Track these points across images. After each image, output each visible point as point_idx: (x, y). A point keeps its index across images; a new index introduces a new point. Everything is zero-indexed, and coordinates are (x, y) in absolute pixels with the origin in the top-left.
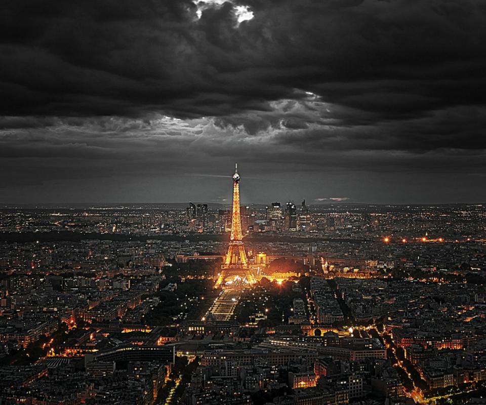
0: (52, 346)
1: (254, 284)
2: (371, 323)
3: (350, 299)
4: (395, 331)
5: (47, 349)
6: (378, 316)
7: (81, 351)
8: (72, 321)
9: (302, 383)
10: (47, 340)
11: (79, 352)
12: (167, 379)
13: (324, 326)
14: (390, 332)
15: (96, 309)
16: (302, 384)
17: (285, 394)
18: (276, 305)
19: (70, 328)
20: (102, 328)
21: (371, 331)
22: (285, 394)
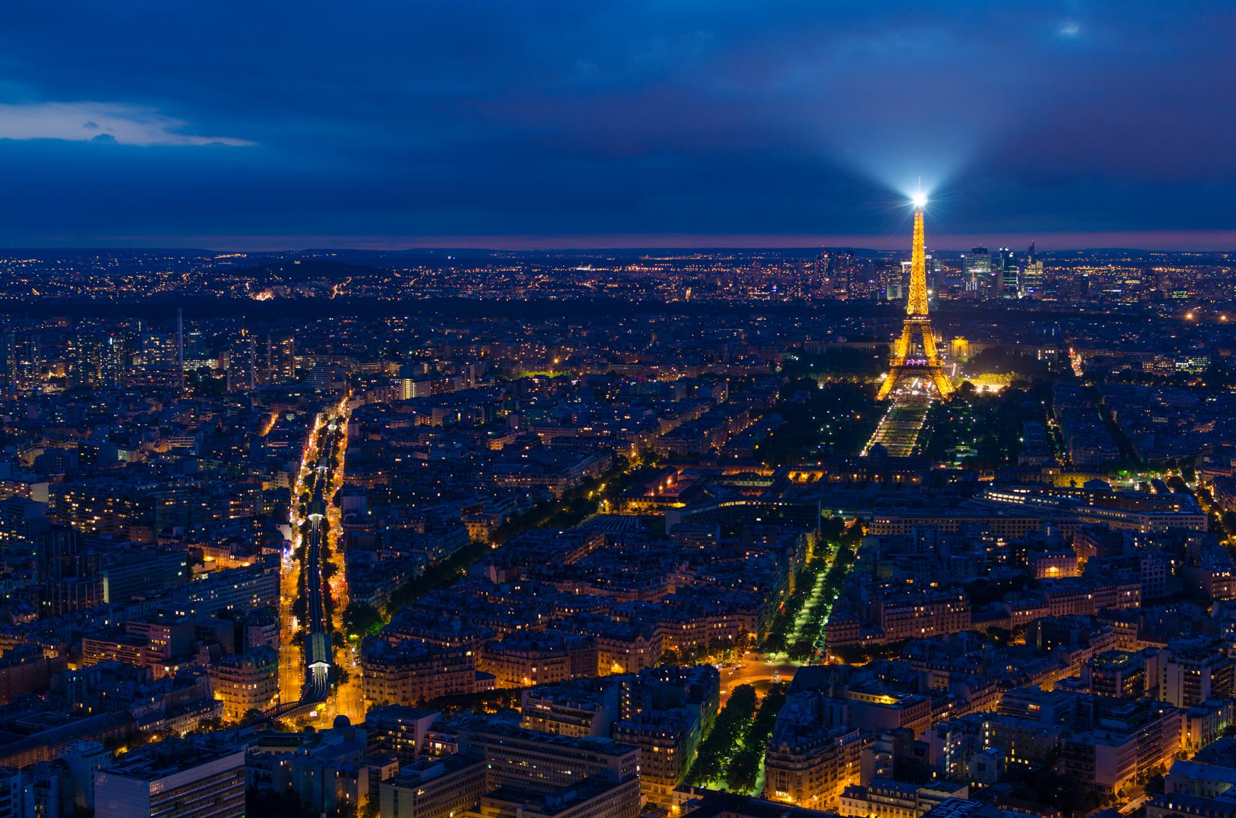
0: (605, 495)
1: (950, 394)
2: (1171, 465)
3: (1129, 423)
4: (1217, 481)
5: (597, 499)
6: (1184, 453)
7: (655, 505)
8: (634, 454)
9: (1053, 569)
10: (594, 485)
11: (651, 507)
12: (810, 556)
13: (1081, 470)
14: (1208, 484)
15: (675, 433)
16: (1053, 571)
17: (1025, 587)
18: (997, 431)
19: (633, 465)
20: (687, 467)
21: (1173, 481)
22: (1025, 587)
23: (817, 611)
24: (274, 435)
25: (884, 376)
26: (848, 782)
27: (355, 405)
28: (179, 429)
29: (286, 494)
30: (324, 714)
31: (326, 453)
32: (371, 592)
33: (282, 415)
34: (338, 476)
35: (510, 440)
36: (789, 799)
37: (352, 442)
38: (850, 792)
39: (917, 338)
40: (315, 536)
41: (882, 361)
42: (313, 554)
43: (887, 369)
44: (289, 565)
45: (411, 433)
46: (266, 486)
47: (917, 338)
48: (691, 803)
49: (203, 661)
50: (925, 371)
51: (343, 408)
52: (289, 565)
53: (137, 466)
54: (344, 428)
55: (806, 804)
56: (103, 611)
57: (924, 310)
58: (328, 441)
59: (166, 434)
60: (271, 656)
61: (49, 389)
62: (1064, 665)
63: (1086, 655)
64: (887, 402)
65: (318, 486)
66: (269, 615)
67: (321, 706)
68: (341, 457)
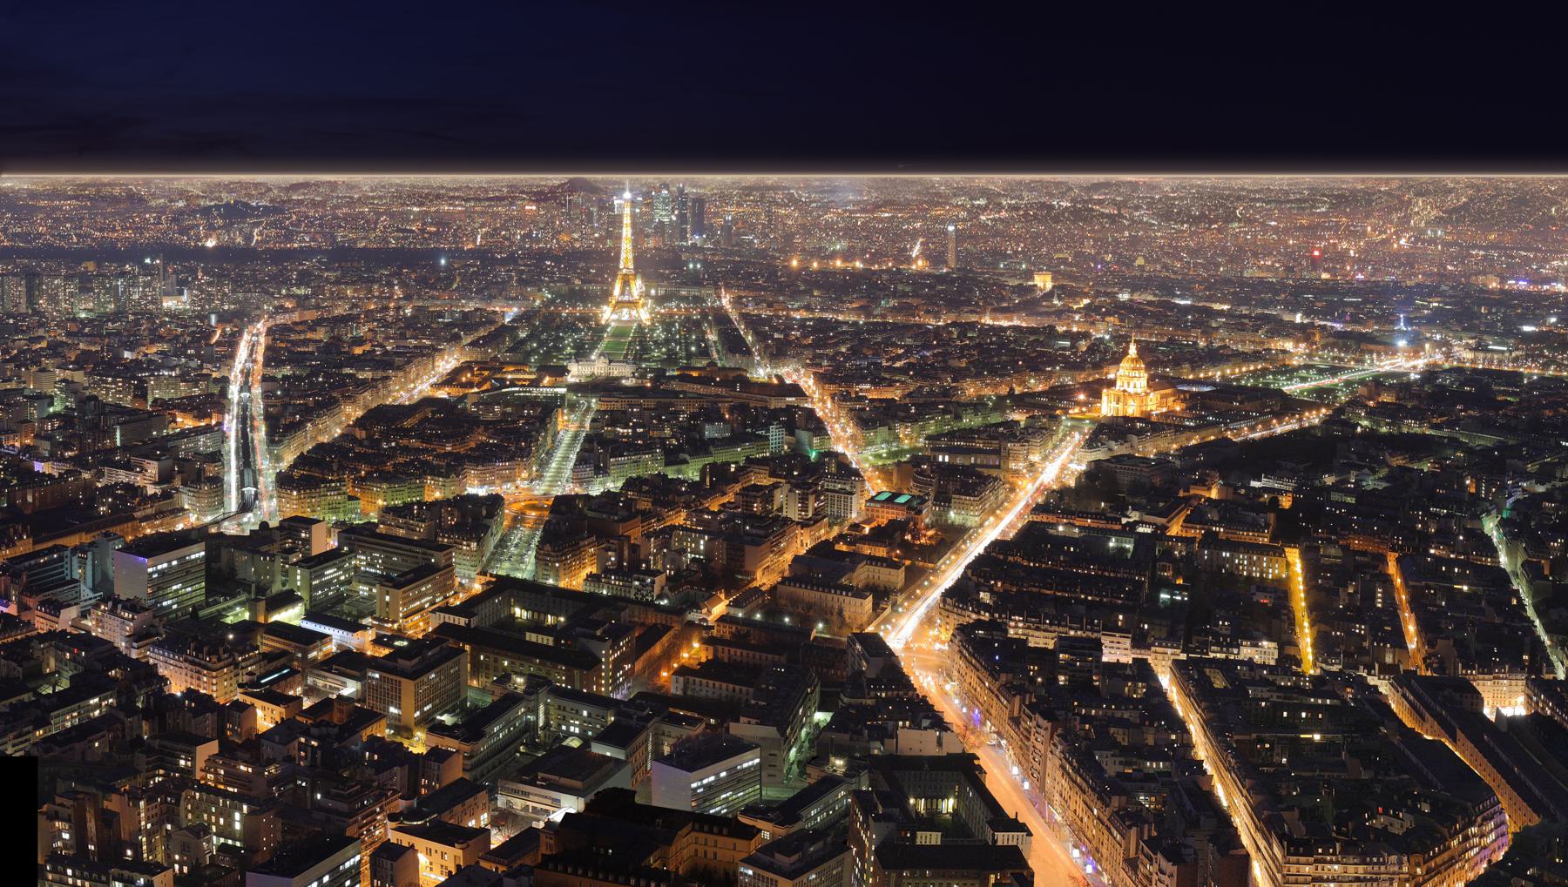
23: (566, 458)
24: (218, 343)
25: (605, 307)
26: (588, 570)
27: (271, 323)
28: (161, 339)
29: (225, 381)
30: (251, 521)
31: (251, 355)
32: (279, 443)
33: (224, 331)
34: (258, 369)
35: (368, 347)
36: (551, 581)
37: (268, 348)
38: (591, 577)
39: (626, 283)
40: (244, 408)
41: (605, 296)
42: (245, 420)
43: (608, 303)
44: (231, 425)
45: (306, 342)
46: (214, 375)
47: (626, 283)
48: (488, 583)
49: (177, 482)
50: (632, 304)
51: (261, 326)
52: (231, 425)
53: (135, 361)
54: (262, 339)
55: (562, 584)
56: (114, 450)
57: (631, 266)
58: (252, 348)
59: (152, 342)
60: (217, 481)
61: (83, 315)
62: (724, 494)
63: (738, 487)
64: (607, 325)
65: (247, 374)
66: (216, 457)
67: (250, 515)
68: (260, 358)
